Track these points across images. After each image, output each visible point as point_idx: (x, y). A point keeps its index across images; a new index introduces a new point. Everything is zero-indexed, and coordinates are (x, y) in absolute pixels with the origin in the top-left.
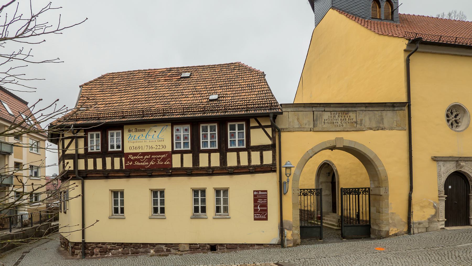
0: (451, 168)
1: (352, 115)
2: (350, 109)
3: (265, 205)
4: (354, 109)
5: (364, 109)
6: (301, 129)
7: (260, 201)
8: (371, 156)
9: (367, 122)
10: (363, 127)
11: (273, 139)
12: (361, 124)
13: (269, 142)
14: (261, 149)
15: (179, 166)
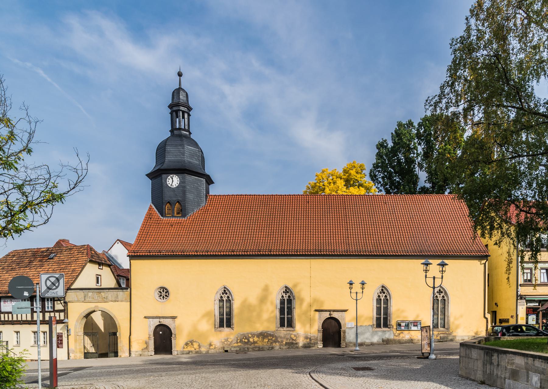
0: (156, 322)
1: (103, 294)
2: (101, 291)
3: (62, 340)
4: (103, 291)
5: (108, 291)
6: (78, 301)
7: (60, 338)
8: (112, 316)
9: (110, 298)
10: (108, 300)
11: (64, 306)
12: (107, 299)
13: (63, 308)
14: (59, 311)
15: (16, 320)
